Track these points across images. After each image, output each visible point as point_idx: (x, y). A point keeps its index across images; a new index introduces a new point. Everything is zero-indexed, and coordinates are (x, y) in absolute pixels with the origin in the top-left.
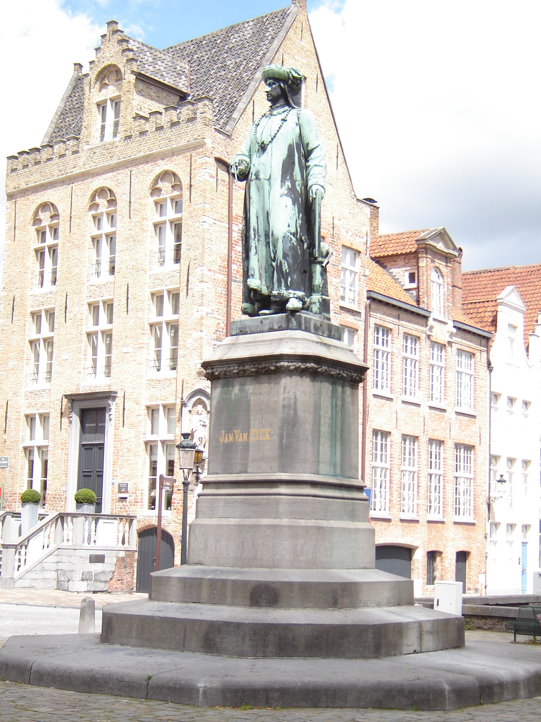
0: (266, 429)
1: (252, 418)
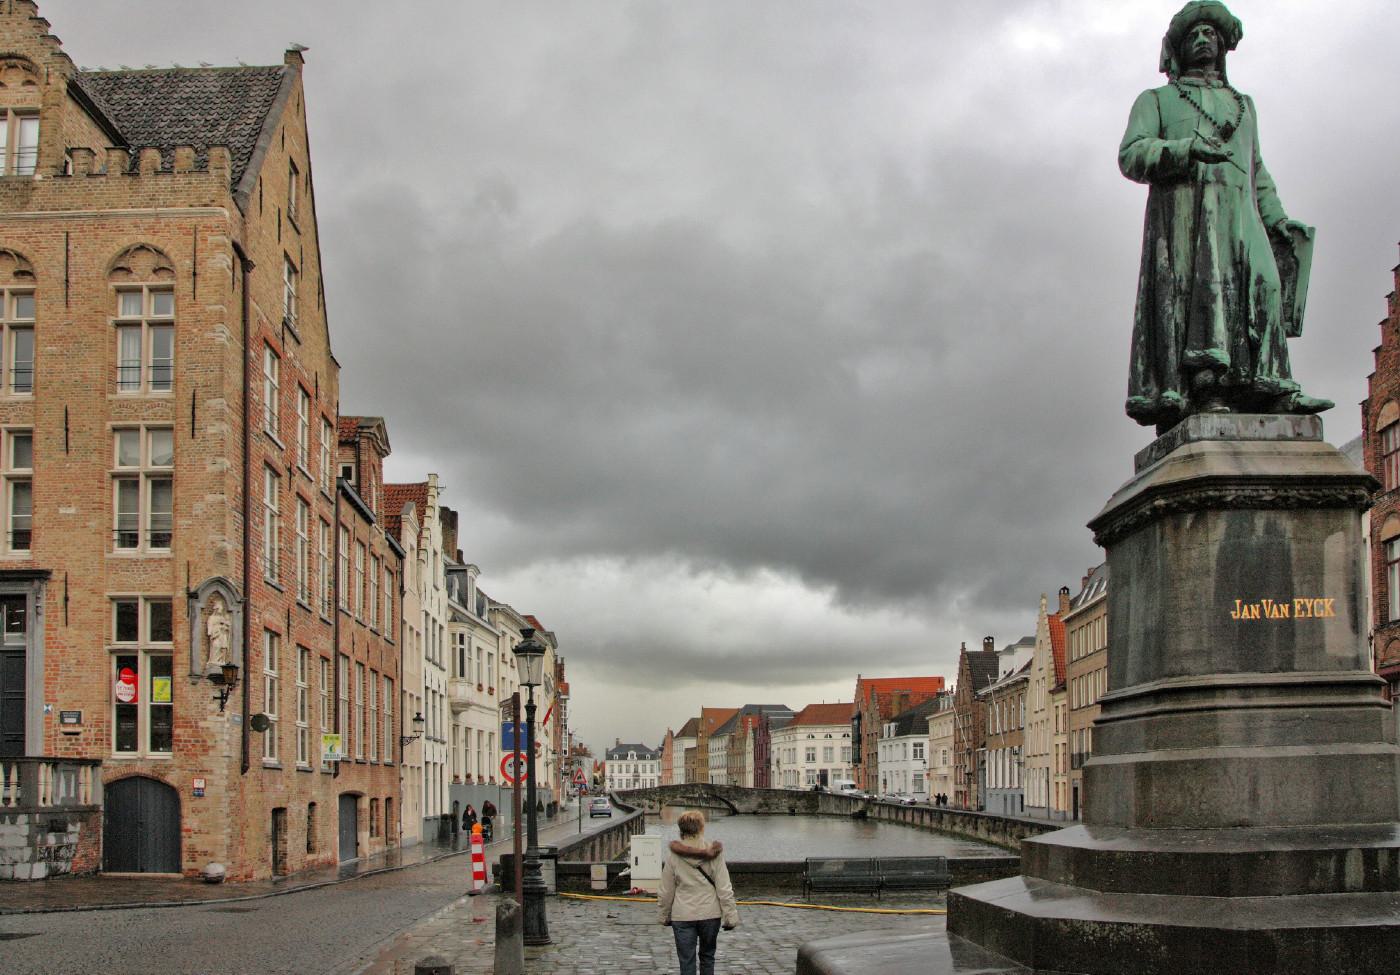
1: (1295, 580)
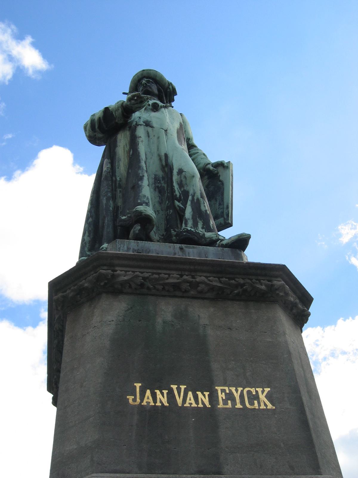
0: (259, 390)
1: (215, 366)
